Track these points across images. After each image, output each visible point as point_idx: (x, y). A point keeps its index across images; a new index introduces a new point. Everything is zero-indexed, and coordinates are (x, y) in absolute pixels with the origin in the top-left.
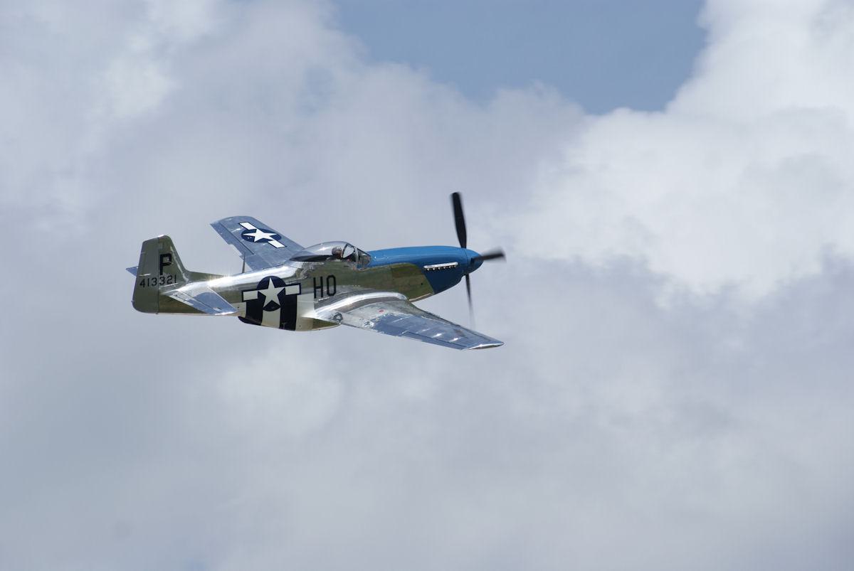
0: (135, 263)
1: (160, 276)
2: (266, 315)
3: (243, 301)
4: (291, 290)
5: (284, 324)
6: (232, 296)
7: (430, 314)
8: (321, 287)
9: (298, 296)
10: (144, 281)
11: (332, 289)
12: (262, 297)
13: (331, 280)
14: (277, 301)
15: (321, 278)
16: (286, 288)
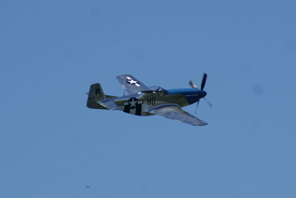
0: (88, 91)
1: (96, 96)
2: (131, 110)
3: (123, 105)
4: (139, 102)
5: (137, 113)
6: (119, 104)
7: (187, 113)
8: (150, 102)
9: (142, 105)
10: (91, 98)
11: (153, 102)
12: (130, 104)
13: (154, 99)
14: (135, 106)
15: (150, 99)
16: (138, 102)
